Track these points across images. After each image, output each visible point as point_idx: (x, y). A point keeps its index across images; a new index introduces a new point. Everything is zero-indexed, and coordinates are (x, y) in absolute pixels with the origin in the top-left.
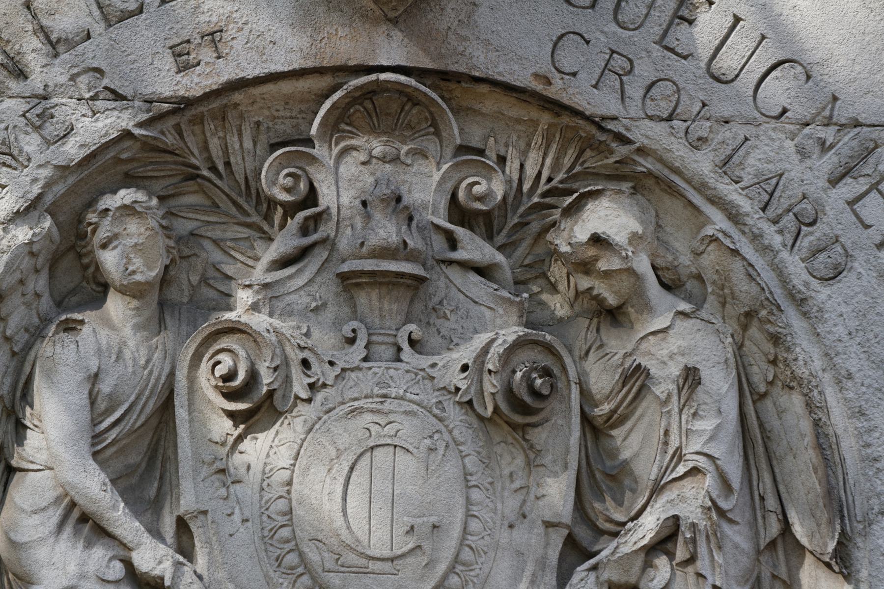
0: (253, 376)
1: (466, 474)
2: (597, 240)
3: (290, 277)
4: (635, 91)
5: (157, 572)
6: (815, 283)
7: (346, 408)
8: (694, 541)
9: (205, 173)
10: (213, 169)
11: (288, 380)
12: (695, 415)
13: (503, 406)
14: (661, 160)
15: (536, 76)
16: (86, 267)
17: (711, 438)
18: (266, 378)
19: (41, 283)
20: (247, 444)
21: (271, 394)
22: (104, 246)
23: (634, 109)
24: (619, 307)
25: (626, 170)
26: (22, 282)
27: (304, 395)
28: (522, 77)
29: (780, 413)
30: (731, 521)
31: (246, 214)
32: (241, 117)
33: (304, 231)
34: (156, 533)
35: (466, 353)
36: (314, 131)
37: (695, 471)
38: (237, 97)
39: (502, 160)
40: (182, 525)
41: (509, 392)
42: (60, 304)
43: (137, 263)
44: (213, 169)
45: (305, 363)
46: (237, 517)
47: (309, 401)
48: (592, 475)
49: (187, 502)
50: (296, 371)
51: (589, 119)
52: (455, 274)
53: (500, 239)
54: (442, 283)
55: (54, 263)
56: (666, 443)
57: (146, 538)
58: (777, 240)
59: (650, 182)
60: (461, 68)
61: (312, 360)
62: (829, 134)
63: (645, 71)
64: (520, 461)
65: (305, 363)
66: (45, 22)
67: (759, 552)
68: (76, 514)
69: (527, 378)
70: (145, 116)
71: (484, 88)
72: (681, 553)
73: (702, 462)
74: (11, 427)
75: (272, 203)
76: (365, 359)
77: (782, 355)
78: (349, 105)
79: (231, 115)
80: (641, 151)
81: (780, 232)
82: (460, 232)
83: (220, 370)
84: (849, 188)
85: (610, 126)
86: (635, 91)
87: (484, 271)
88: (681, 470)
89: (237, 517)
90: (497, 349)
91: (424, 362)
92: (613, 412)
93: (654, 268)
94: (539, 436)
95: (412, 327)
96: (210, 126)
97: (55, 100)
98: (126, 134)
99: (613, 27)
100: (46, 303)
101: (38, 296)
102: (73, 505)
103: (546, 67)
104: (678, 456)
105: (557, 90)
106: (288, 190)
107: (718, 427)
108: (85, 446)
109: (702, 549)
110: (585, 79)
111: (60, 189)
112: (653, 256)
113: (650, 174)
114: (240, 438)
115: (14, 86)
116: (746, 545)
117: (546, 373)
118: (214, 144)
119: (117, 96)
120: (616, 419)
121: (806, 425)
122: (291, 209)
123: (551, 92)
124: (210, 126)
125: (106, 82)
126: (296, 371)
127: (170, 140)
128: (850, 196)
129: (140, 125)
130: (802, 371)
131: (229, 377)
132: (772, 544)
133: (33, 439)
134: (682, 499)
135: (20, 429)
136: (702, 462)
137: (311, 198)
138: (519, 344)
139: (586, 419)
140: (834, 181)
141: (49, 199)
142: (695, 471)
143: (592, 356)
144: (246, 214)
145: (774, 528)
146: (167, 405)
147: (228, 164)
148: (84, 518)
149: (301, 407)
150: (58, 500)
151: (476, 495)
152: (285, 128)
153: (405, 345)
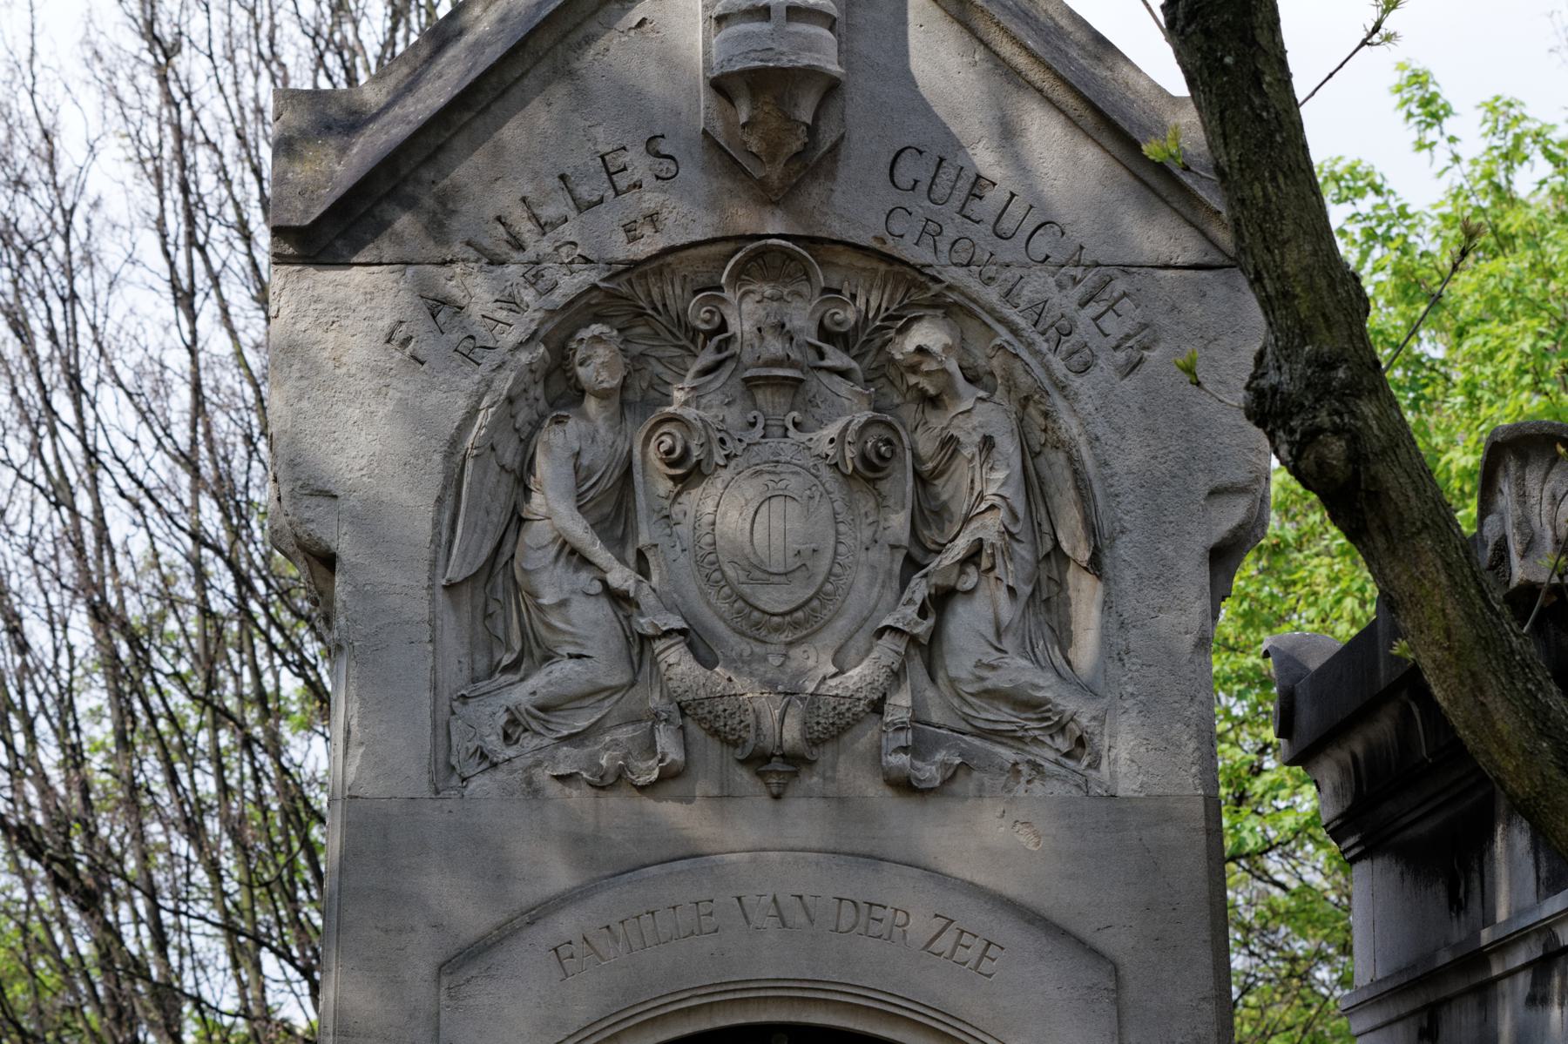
0: (686, 451)
1: (835, 514)
2: (921, 350)
3: (710, 382)
4: (944, 246)
5: (624, 587)
6: (1071, 375)
7: (751, 471)
8: (993, 555)
9: (650, 312)
10: (655, 309)
11: (710, 453)
12: (992, 468)
13: (859, 466)
14: (963, 294)
15: (876, 238)
16: (569, 379)
17: (1003, 484)
18: (696, 453)
19: (538, 391)
20: (684, 498)
21: (699, 462)
22: (581, 364)
23: (944, 259)
24: (938, 396)
25: (940, 301)
26: (525, 390)
27: (722, 463)
28: (865, 239)
29: (1050, 465)
30: (1019, 541)
31: (678, 338)
32: (673, 272)
33: (719, 349)
34: (623, 561)
35: (833, 430)
36: (723, 280)
37: (992, 507)
38: (670, 259)
39: (854, 297)
40: (641, 556)
41: (864, 458)
42: (552, 405)
43: (604, 375)
44: (655, 309)
45: (722, 441)
46: (678, 548)
47: (725, 466)
48: (922, 512)
49: (644, 539)
50: (716, 447)
51: (913, 267)
52: (823, 376)
53: (854, 351)
54: (815, 383)
55: (547, 376)
56: (972, 488)
57: (616, 565)
58: (1045, 346)
59: (956, 309)
60: (824, 235)
61: (727, 438)
62: (1078, 272)
63: (950, 233)
64: (872, 504)
65: (722, 441)
66: (536, 211)
67: (1038, 562)
68: (567, 549)
69: (875, 446)
70: (607, 274)
71: (839, 248)
72: (985, 563)
73: (997, 501)
74: (521, 491)
75: (696, 331)
76: (764, 437)
77: (1051, 425)
78: (747, 262)
79: (666, 271)
80: (950, 288)
81: (1047, 341)
82: (826, 347)
83: (663, 448)
84: (1093, 309)
85: (928, 271)
86: (944, 246)
87: (844, 374)
88: (983, 506)
89: (678, 548)
90: (854, 427)
91: (804, 437)
92: (935, 468)
93: (961, 368)
94: (884, 486)
95: (795, 414)
96: (652, 280)
97: (545, 265)
98: (594, 287)
99: (927, 203)
100: (542, 405)
101: (537, 400)
102: (565, 543)
103: (882, 232)
104: (981, 497)
105: (891, 247)
106: (707, 322)
107: (1008, 477)
108: (572, 503)
109: (999, 561)
110: (909, 240)
111: (550, 326)
112: (960, 360)
113: (955, 303)
114: (679, 494)
115: (516, 255)
116: (1028, 556)
117: (888, 442)
118: (655, 292)
119: (587, 261)
120: (938, 473)
121: (1067, 474)
122: (709, 335)
123: (885, 249)
124: (652, 280)
125: (579, 251)
126: (716, 447)
127: (625, 289)
128: (1094, 315)
129: (604, 280)
130: (1064, 436)
131: (670, 451)
132: (1047, 556)
133: (537, 499)
134: (984, 527)
135: (527, 492)
136: (997, 501)
137: (723, 327)
138: (869, 423)
139: (917, 474)
140: (1083, 305)
141: (542, 333)
142: (992, 507)
143: (919, 430)
144: (678, 338)
145: (1049, 545)
146: (628, 473)
147: (665, 305)
148: (573, 552)
149: (721, 472)
150: (554, 540)
151: (842, 528)
152: (703, 279)
153: (790, 426)
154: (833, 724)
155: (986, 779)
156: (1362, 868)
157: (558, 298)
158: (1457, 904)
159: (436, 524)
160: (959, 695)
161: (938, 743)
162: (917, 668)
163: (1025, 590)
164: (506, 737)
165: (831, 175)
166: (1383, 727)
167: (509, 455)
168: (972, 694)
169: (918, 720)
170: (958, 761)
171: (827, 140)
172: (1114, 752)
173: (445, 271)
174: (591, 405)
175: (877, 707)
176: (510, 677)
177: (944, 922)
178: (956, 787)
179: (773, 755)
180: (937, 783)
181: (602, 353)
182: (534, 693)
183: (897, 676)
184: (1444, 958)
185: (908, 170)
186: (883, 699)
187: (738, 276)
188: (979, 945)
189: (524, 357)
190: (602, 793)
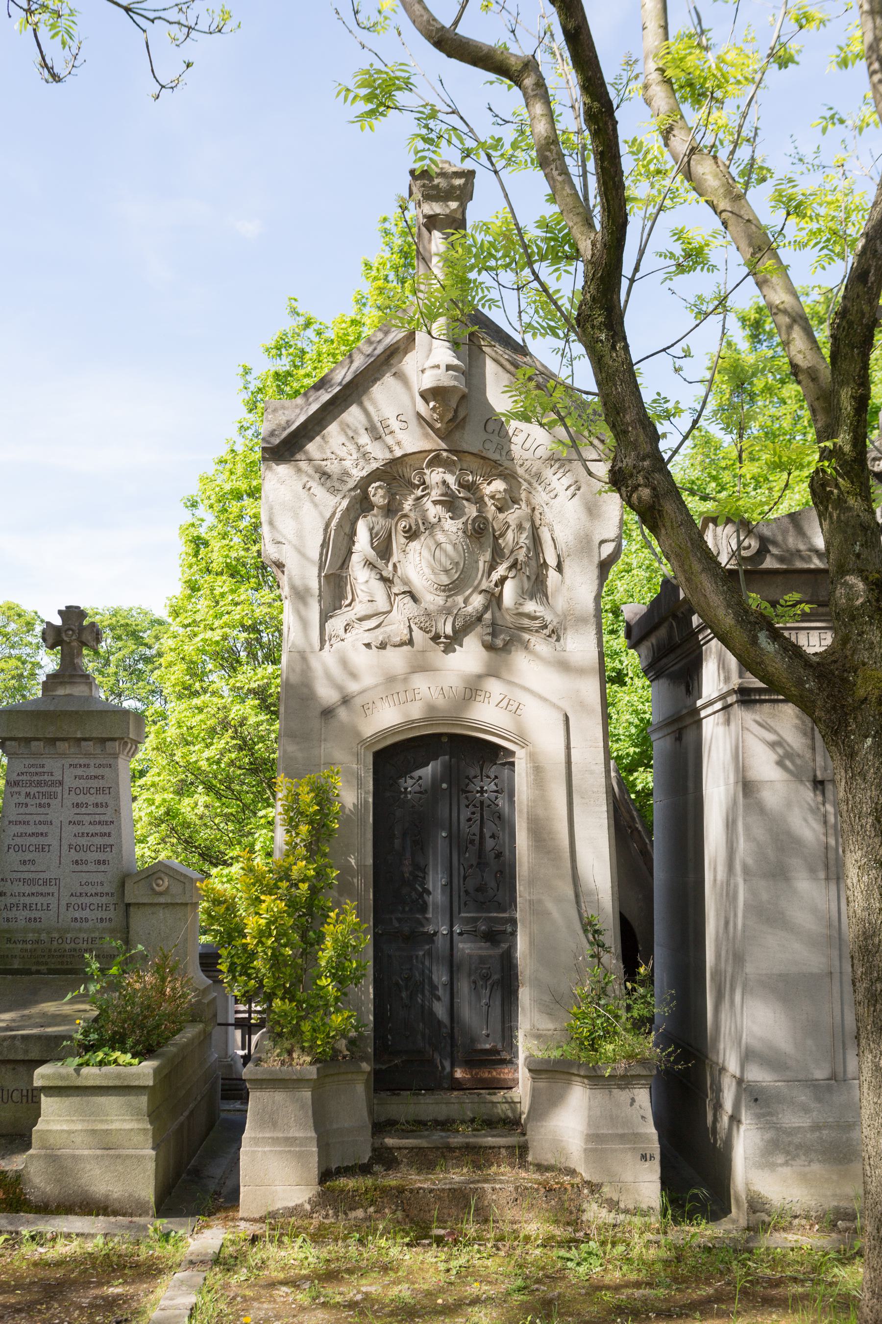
0: (410, 527)
18: (414, 527)
19: (358, 506)
28: (475, 451)
41: (474, 528)
42: (363, 512)
72: (519, 567)
86: (504, 453)
104: (517, 543)
110: (492, 451)
135: (354, 542)
137: (424, 483)
146: (390, 535)
152: (417, 466)
156: (656, 682)
157: (364, 473)
158: (689, 692)
159: (321, 554)
162: (494, 602)
163: (533, 578)
165: (463, 428)
166: (662, 632)
167: (347, 530)
169: (494, 624)
171: (461, 415)
173: (324, 463)
174: (375, 511)
175: (479, 619)
176: (348, 609)
181: (381, 492)
183: (486, 608)
184: (684, 712)
185: (491, 426)
186: (482, 616)
187: (431, 464)
189: (353, 493)
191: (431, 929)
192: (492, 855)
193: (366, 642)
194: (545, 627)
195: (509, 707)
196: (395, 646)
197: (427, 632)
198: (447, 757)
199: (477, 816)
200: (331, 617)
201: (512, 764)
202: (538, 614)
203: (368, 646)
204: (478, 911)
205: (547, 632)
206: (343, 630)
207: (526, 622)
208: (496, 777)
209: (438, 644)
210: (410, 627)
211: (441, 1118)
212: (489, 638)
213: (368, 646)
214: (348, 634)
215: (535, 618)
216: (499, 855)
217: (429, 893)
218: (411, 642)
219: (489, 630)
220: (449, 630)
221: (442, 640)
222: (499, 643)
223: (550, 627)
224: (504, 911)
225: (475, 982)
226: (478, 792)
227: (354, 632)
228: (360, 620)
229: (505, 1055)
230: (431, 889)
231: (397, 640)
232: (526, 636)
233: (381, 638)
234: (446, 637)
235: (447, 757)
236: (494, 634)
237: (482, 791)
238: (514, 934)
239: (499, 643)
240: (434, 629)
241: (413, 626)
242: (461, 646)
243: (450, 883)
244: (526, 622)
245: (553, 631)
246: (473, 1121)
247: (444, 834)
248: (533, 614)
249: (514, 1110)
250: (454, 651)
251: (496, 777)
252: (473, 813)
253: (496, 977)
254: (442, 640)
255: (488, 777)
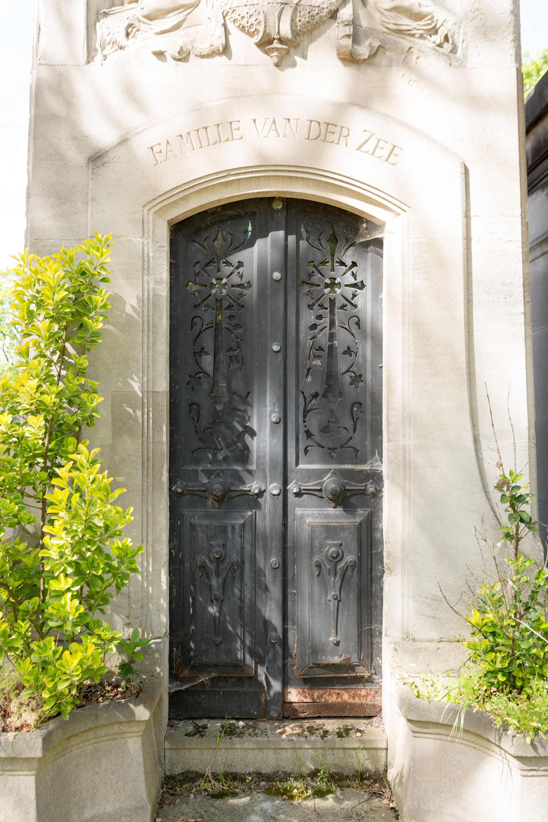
154: (308, 22)
155: (394, 56)
160: (379, 11)
161: (367, 36)
164: (128, 35)
168: (387, 10)
169: (354, 23)
170: (378, 44)
172: (465, 43)
175: (333, 15)
177: (369, 134)
178: (377, 60)
179: (274, 39)
180: (367, 57)
182: (143, 9)
186: (337, 11)
188: (389, 148)
190: (179, 63)
191: (254, 486)
192: (347, 378)
193: (157, 49)
194: (435, 31)
195: (378, 152)
196: (203, 57)
197: (251, 35)
198: (281, 233)
199: (326, 321)
200: (106, 14)
201: (379, 243)
202: (424, 10)
203: (160, 55)
204: (324, 462)
205: (438, 38)
206: (124, 34)
207: (406, 23)
208: (354, 264)
209: (267, 53)
210: (225, 25)
211: (267, 769)
212: (348, 42)
213: (160, 55)
214: (131, 40)
215: (418, 17)
216: (358, 378)
217: (253, 434)
218: (226, 50)
219: (349, 30)
220: (286, 31)
221: (276, 44)
222: (363, 51)
223: (442, 32)
224: (364, 462)
225: (319, 566)
226: (327, 286)
227: (139, 35)
228: (150, 17)
229: (362, 672)
230: (255, 427)
231: (204, 47)
232: (406, 43)
233: (180, 43)
234: (281, 41)
235: (281, 233)
236: (356, 38)
237: (333, 285)
238: (377, 495)
239: (363, 51)
240: (261, 28)
241: (230, 25)
242: (305, 57)
243: (284, 420)
244: (406, 23)
245: (446, 38)
246: (314, 774)
247: (276, 348)
248: (416, 9)
249: (375, 761)
250: (294, 65)
251: (354, 264)
252: (320, 317)
253: (350, 558)
254: (276, 44)
255: (342, 264)
